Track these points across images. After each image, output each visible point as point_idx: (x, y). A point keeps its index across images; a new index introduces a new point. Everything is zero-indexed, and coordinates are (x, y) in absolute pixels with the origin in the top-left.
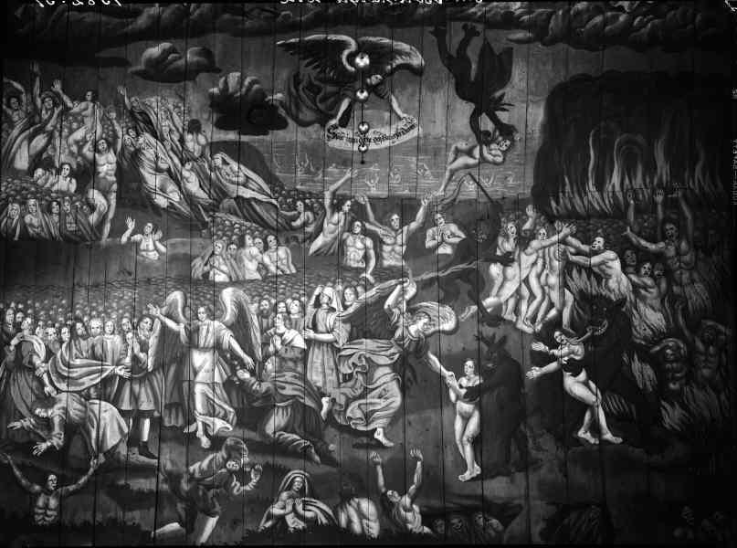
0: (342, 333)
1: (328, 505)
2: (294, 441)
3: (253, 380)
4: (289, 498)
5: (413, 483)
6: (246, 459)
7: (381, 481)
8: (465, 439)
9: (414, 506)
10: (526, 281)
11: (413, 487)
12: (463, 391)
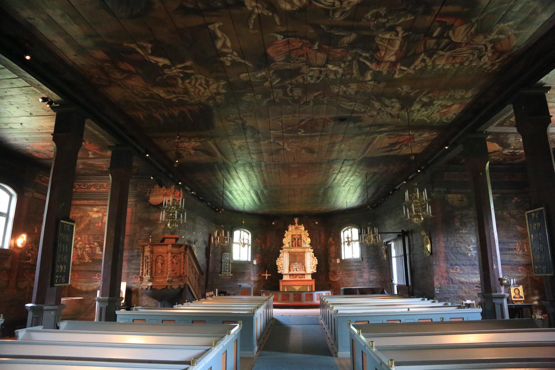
0: (305, 69)
1: (316, 6)
2: (339, 32)
3: (361, 53)
4: (345, 8)
5: (254, 19)
6: (372, 23)
7: (277, 19)
8: (223, 39)
9: (251, 9)
10: (205, 89)
11: (254, 17)
12: (229, 55)
